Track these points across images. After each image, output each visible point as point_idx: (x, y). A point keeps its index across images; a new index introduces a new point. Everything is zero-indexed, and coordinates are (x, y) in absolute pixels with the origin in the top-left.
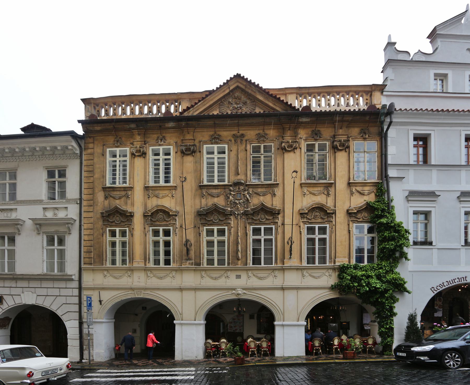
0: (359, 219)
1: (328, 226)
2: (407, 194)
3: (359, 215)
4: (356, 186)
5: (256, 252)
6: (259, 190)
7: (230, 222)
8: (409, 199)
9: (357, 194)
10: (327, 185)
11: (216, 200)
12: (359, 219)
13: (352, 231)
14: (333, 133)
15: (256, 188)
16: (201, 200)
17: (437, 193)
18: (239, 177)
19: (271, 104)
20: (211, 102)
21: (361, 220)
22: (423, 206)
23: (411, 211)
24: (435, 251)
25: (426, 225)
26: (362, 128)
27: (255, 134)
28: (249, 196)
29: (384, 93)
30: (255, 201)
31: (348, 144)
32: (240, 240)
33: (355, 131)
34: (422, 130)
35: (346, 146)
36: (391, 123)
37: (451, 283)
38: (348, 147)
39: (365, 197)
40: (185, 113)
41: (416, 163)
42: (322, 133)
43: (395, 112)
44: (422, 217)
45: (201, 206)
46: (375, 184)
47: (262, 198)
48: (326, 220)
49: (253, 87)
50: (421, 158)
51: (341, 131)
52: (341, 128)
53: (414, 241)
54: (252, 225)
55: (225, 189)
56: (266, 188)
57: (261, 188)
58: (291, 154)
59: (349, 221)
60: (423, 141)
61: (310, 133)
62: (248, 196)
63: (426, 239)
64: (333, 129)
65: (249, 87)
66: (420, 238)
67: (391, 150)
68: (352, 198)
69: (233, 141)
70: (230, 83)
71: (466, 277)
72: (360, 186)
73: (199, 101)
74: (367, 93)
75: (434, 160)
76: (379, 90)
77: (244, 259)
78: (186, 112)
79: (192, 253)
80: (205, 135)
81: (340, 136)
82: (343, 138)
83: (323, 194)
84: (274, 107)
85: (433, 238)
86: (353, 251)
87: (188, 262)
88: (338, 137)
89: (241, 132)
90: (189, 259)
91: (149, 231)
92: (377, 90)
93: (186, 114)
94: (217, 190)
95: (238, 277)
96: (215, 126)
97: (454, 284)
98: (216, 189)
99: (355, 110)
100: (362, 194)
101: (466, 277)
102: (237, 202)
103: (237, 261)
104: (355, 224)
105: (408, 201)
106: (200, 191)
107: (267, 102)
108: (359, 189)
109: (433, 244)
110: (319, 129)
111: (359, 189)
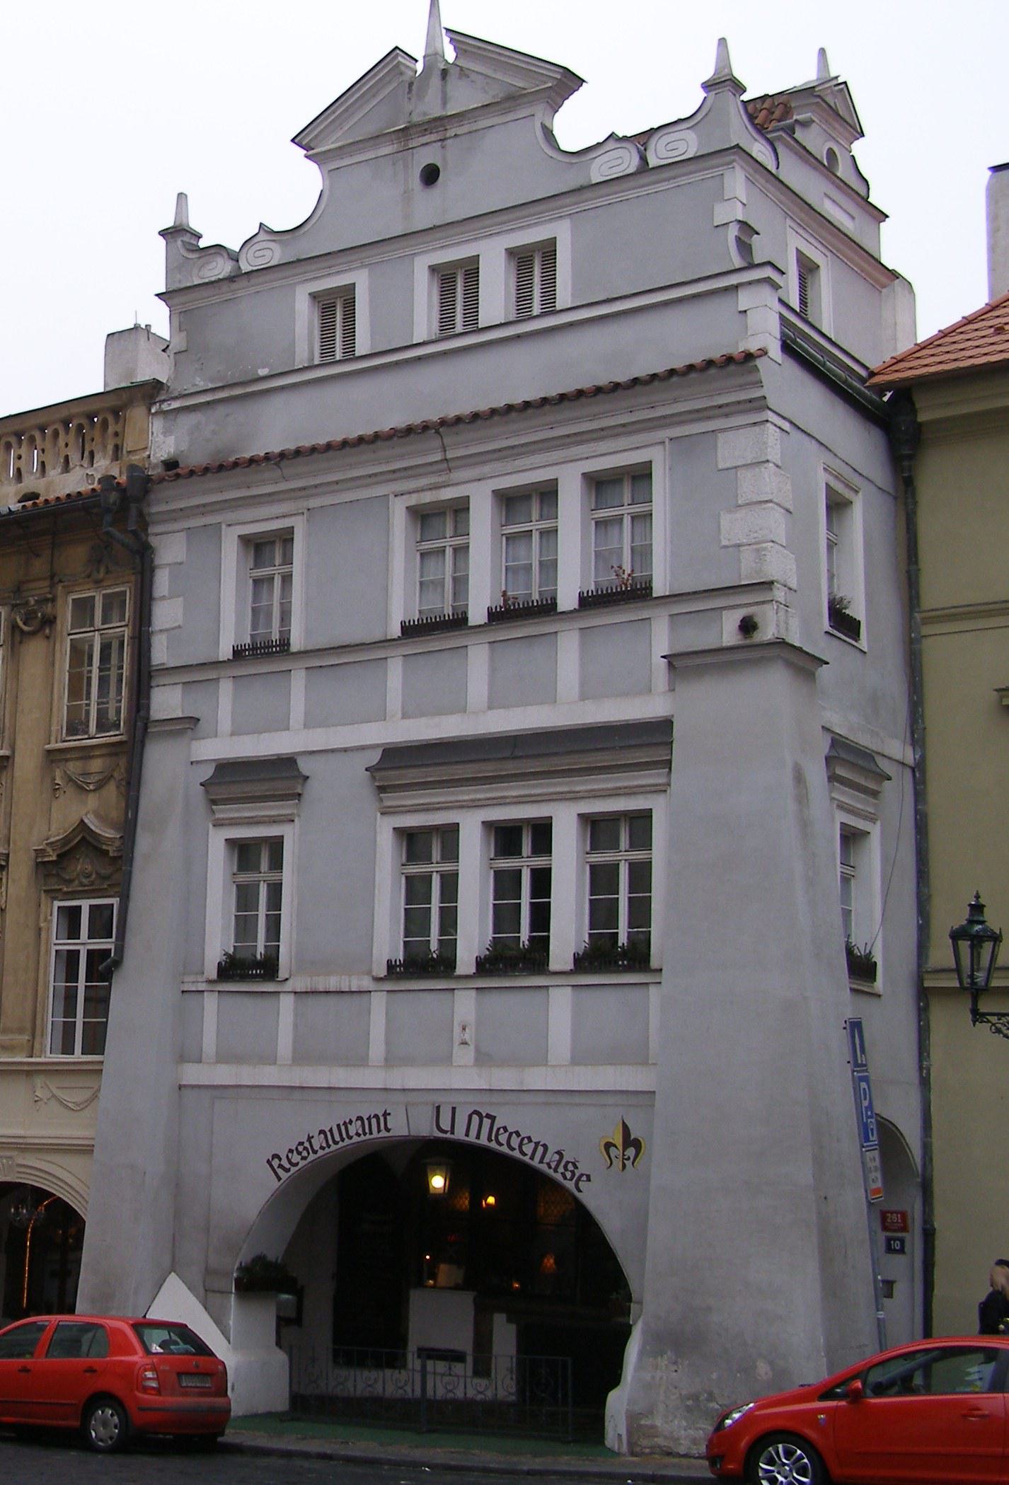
37: (337, 1138)
71: (386, 1114)
101: (386, 1114)
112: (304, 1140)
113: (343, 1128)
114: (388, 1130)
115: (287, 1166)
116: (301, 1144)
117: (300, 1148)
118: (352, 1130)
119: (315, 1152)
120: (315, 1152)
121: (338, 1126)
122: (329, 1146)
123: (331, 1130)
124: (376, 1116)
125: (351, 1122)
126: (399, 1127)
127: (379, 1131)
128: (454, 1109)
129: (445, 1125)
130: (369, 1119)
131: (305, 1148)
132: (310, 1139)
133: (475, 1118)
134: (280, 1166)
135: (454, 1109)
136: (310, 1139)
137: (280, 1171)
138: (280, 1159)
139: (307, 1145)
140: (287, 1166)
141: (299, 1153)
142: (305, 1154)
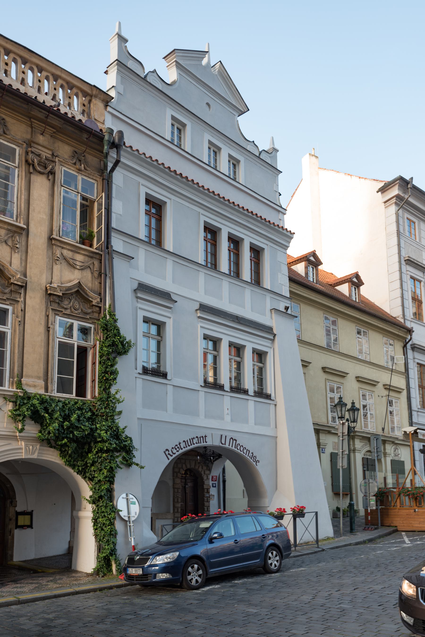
0: (66, 309)
1: (10, 308)
2: (135, 286)
3: (66, 302)
4: (63, 248)
8: (139, 295)
9: (64, 264)
10: (14, 229)
12: (66, 309)
13: (54, 329)
14: (29, 137)
17: (174, 297)
21: (68, 312)
22: (157, 313)
23: (141, 314)
24: (170, 389)
25: (159, 343)
26: (76, 150)
29: (109, 109)
31: (53, 168)
33: (65, 150)
34: (159, 194)
35: (49, 169)
36: (117, 163)
37: (190, 444)
38: (52, 173)
39: (76, 271)
41: (146, 240)
42: (9, 125)
43: (124, 147)
44: (154, 329)
46: (91, 255)
48: (8, 296)
50: (153, 236)
51: (41, 139)
52: (42, 134)
53: (144, 367)
59: (47, 308)
60: (156, 208)
63: (159, 367)
64: (29, 129)
66: (152, 363)
67: (117, 206)
71: (206, 436)
72: (69, 250)
74: (85, 94)
75: (169, 243)
76: (103, 101)
81: (40, 148)
82: (46, 154)
83: (4, 244)
85: (169, 367)
86: (53, 369)
88: (36, 146)
92: (100, 99)
97: (193, 446)
99: (66, 113)
100: (72, 266)
101: (206, 436)
104: (58, 318)
105: (137, 298)
108: (67, 253)
109: (169, 377)
111: (67, 253)
112: (178, 444)
113: (191, 440)
114: (206, 442)
115: (172, 454)
116: (176, 445)
117: (176, 447)
118: (195, 441)
119: (182, 449)
120: (182, 449)
121: (190, 439)
122: (187, 447)
123: (187, 441)
124: (202, 437)
125: (194, 438)
126: (209, 442)
127: (203, 442)
128: (226, 436)
129: (223, 442)
130: (200, 438)
131: (178, 447)
132: (180, 444)
133: (231, 440)
134: (169, 454)
135: (226, 436)
136: (180, 444)
137: (169, 456)
138: (169, 451)
139: (179, 446)
140: (172, 454)
141: (176, 449)
142: (178, 449)
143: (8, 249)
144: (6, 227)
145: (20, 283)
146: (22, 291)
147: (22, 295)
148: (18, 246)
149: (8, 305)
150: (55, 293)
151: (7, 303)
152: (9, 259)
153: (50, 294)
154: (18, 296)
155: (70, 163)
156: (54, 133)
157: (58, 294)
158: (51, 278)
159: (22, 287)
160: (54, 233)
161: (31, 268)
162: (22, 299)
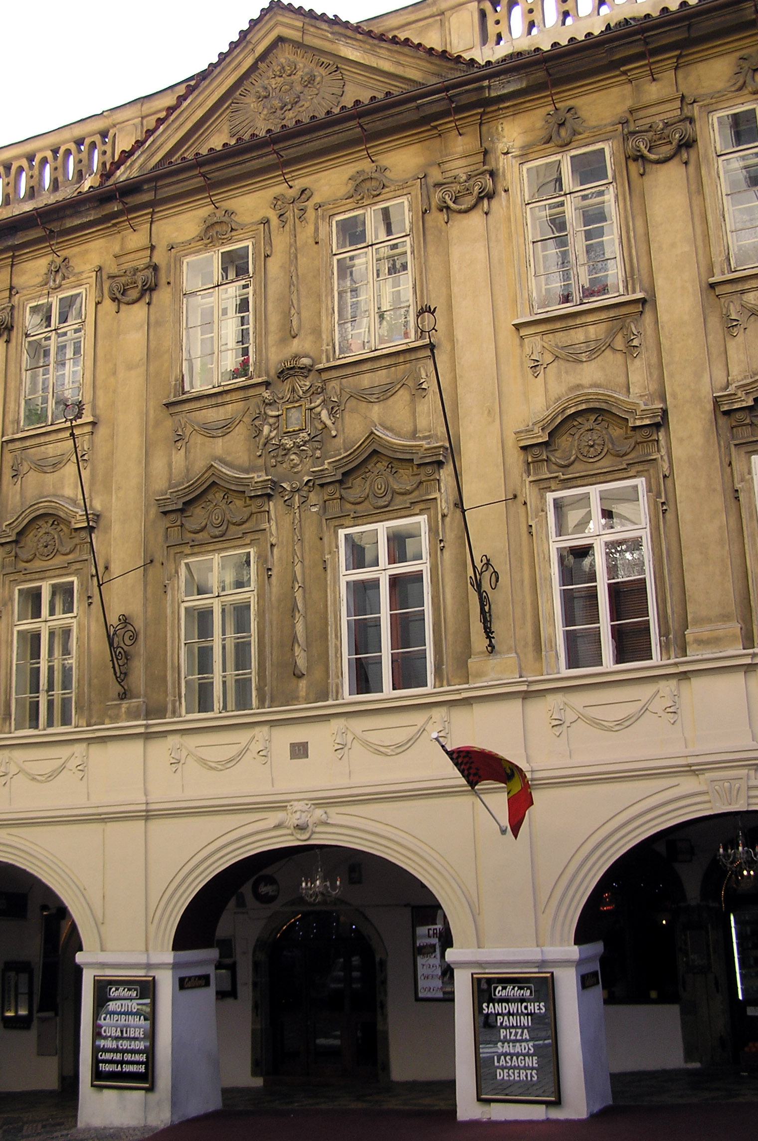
5: (364, 636)
6: (366, 380)
7: (265, 526)
11: (219, 446)
15: (353, 375)
16: (170, 455)
18: (296, 346)
19: (386, 66)
20: (200, 114)
27: (346, 177)
28: (331, 413)
30: (353, 428)
32: (299, 595)
40: (118, 173)
45: (170, 480)
47: (376, 411)
49: (324, 26)
54: (342, 526)
55: (246, 399)
56: (388, 367)
57: (372, 370)
58: (475, 219)
61: (539, 124)
62: (324, 414)
65: (312, 29)
68: (732, 345)
69: (275, 221)
70: (253, 37)
73: (160, 121)
77: (318, 674)
78: (122, 168)
79: (138, 668)
80: (182, 224)
82: (672, 111)
84: (399, 71)
87: (125, 705)
89: (299, 184)
90: (124, 695)
91: (11, 599)
93: (122, 175)
94: (221, 409)
95: (300, 750)
96: (211, 186)
98: (217, 405)
102: (288, 442)
103: (294, 680)
106: (169, 423)
107: (373, 62)
110: (570, 103)
143: (619, 357)
144: (603, 315)
145: (647, 422)
146: (661, 435)
147: (662, 442)
148: (635, 343)
149: (634, 477)
150: (736, 406)
151: (631, 474)
152: (622, 380)
153: (727, 413)
154: (652, 448)
155: (730, 95)
156: (679, 57)
157: (744, 404)
158: (725, 374)
159: (657, 426)
160: (717, 270)
161: (672, 376)
162: (663, 452)
